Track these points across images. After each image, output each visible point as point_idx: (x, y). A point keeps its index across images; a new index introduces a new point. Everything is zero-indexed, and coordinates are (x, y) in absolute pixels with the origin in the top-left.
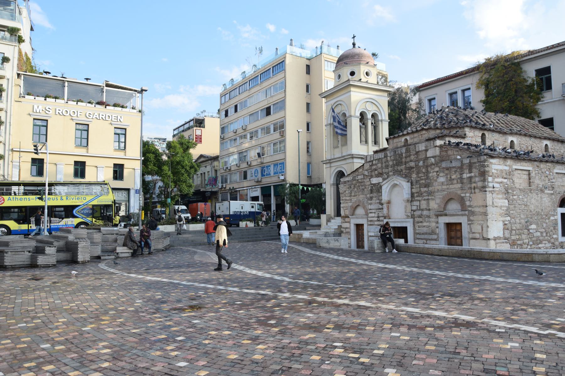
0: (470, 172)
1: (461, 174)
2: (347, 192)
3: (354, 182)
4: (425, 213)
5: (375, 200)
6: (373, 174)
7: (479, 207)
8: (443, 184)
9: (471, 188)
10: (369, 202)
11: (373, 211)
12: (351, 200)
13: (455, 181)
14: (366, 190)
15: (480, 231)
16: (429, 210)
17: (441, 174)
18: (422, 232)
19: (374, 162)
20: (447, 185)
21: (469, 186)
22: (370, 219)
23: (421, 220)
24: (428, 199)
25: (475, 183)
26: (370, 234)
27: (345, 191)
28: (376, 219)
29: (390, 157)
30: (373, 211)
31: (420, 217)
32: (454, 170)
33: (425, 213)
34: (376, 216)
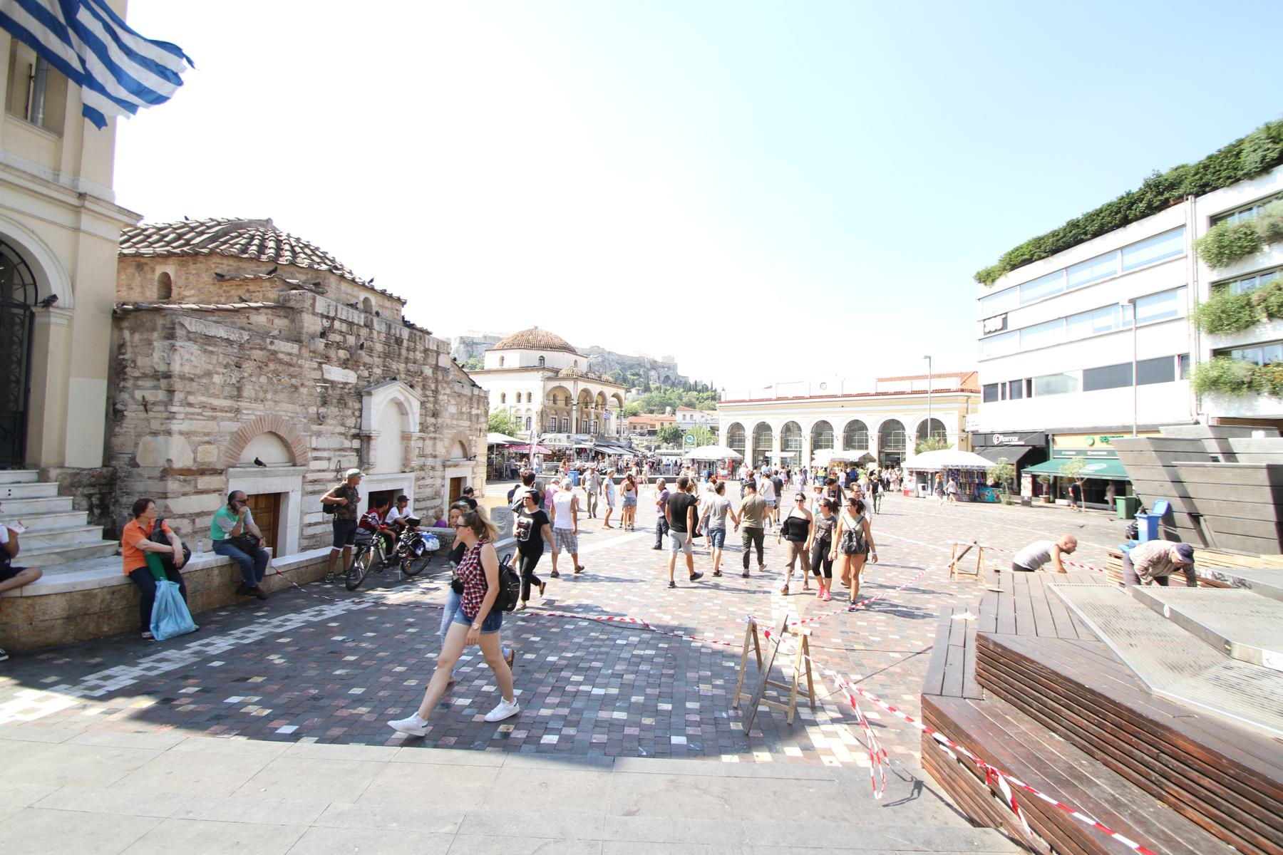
2: (217, 379)
3: (257, 354)
4: (430, 461)
5: (331, 426)
6: (332, 353)
8: (452, 416)
10: (315, 428)
11: (325, 454)
12: (238, 411)
14: (304, 391)
16: (435, 457)
17: (453, 401)
18: (422, 496)
19: (337, 324)
22: (310, 477)
23: (422, 474)
26: (309, 519)
27: (209, 374)
28: (331, 475)
29: (379, 333)
30: (325, 454)
31: (422, 468)
33: (430, 461)
34: (333, 466)
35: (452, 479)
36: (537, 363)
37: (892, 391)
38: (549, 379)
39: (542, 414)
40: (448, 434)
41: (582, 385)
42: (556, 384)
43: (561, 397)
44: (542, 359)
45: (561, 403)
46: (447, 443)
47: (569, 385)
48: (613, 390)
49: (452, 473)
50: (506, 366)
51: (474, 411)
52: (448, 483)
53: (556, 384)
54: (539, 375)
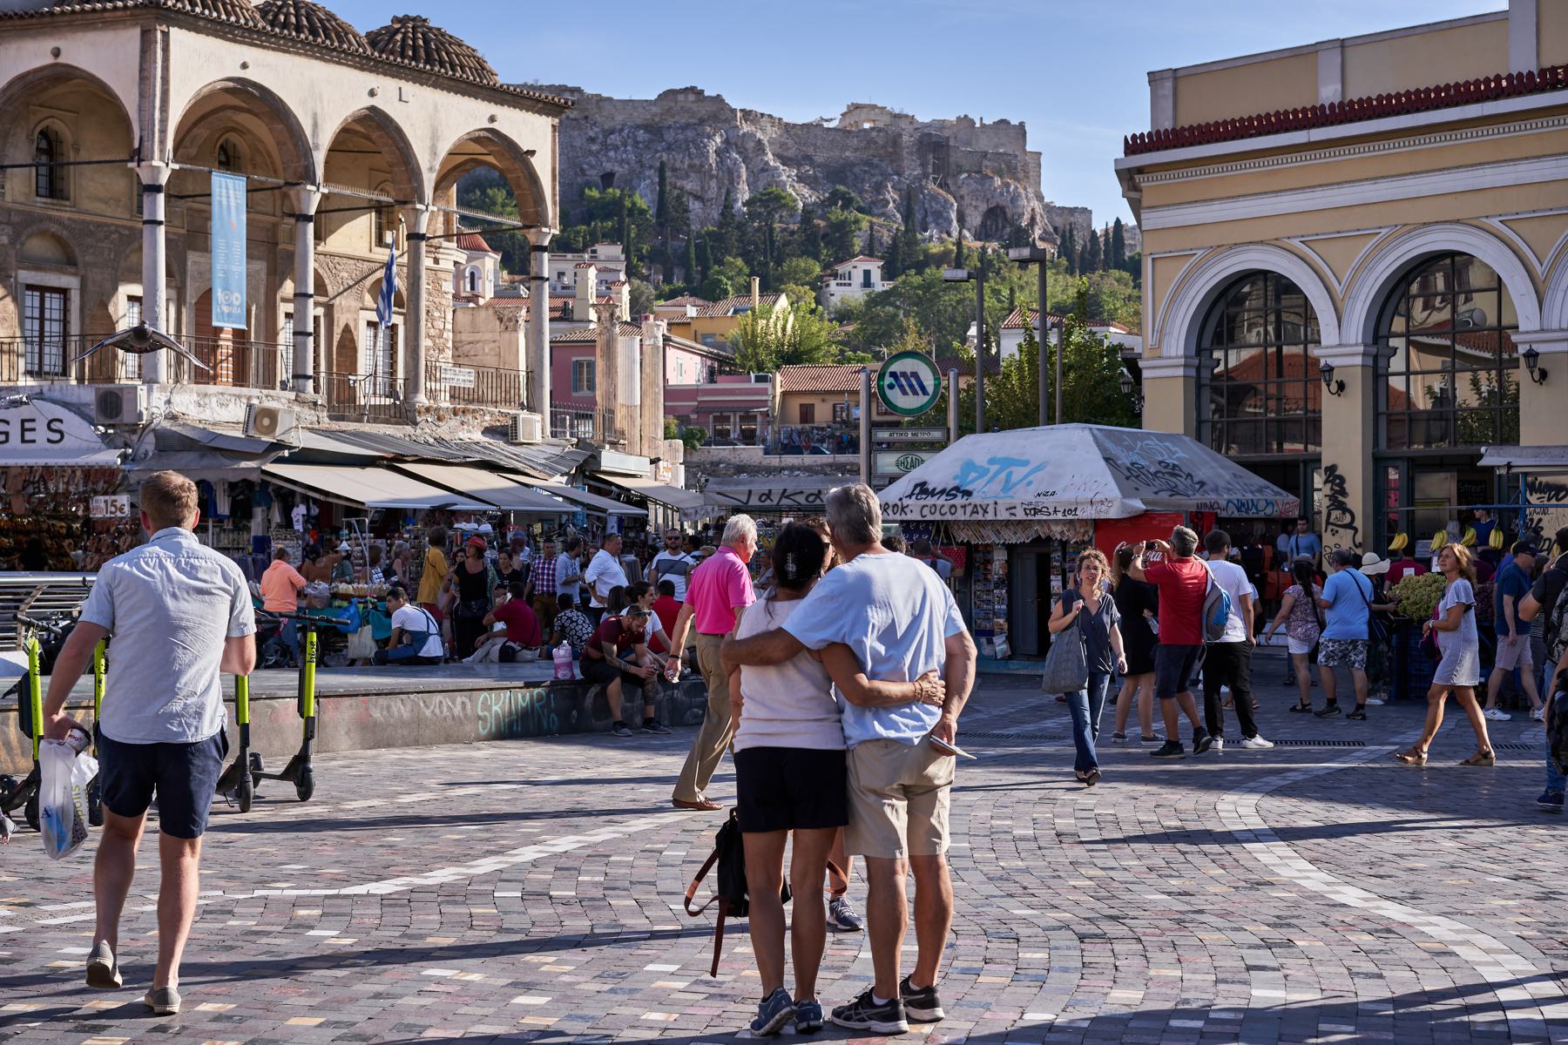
43: (87, 142)
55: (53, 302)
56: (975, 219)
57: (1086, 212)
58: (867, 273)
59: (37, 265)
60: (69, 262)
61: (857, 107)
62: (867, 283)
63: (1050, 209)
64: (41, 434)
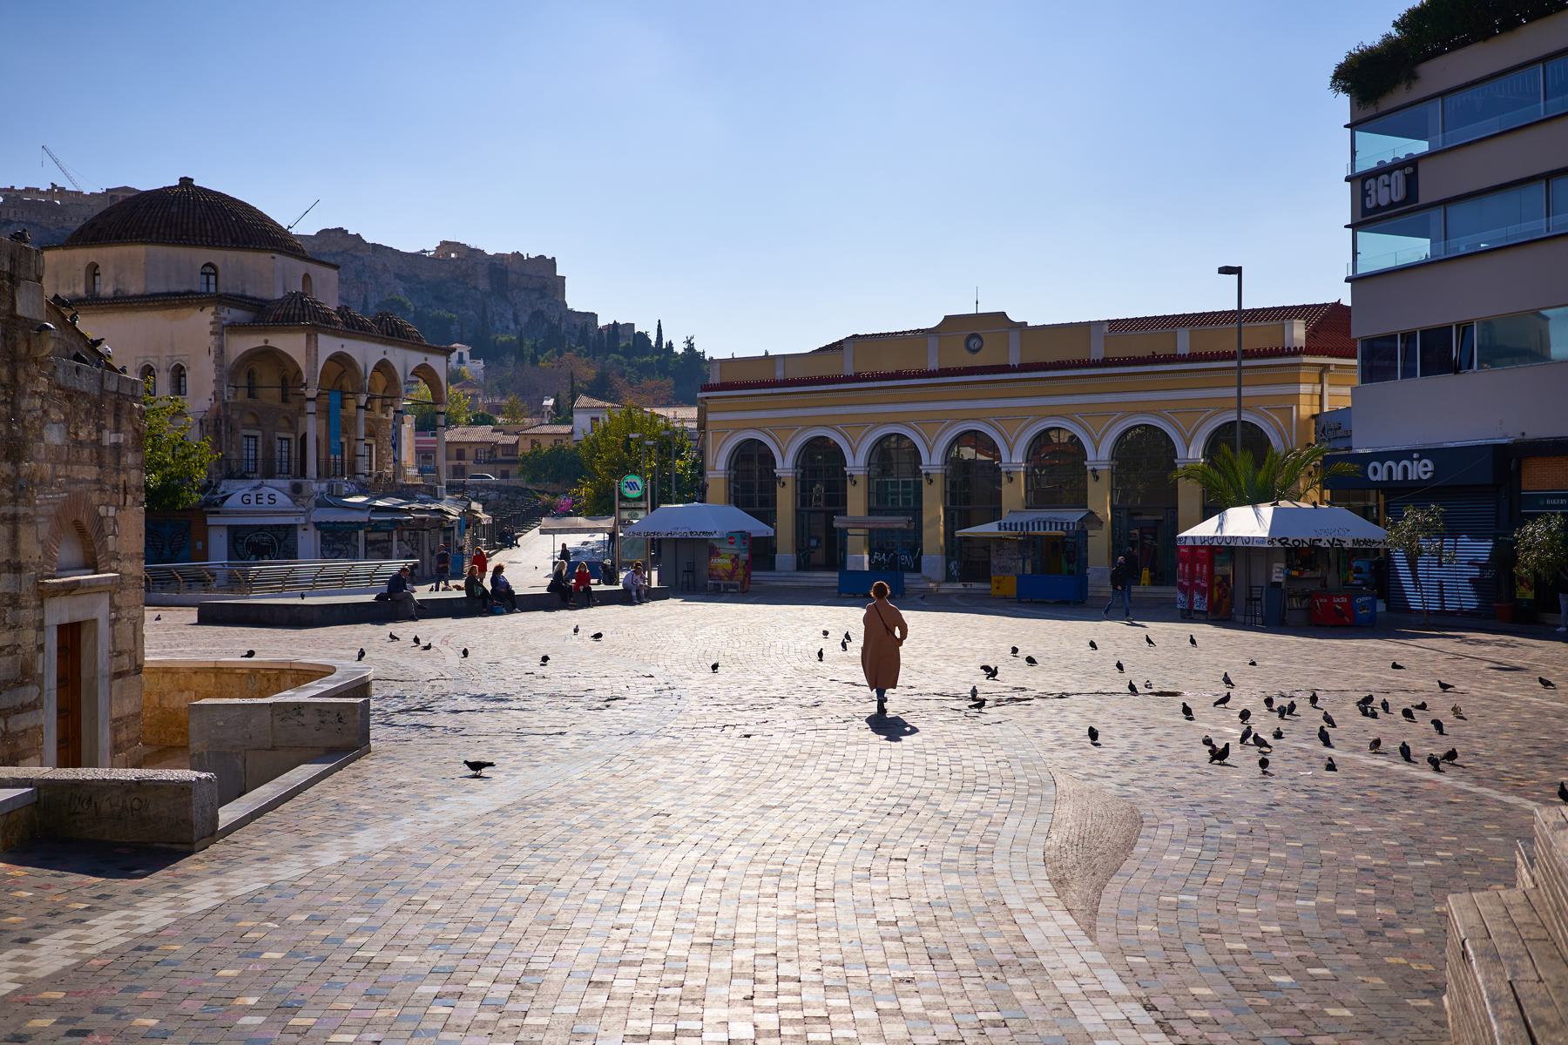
0: (117, 430)
1: (100, 429)
7: (130, 558)
8: (56, 456)
9: (116, 487)
13: (86, 453)
15: (132, 646)
17: (55, 414)
20: (67, 463)
21: (113, 480)
24: (14, 519)
25: (124, 470)
32: (84, 405)
35: (61, 628)
36: (198, 285)
37: (1145, 352)
38: (235, 328)
39: (217, 424)
40: (45, 501)
41: (328, 345)
42: (255, 341)
44: (210, 270)
45: (270, 395)
46: (44, 530)
47: (291, 344)
48: (416, 358)
49: (60, 612)
50: (106, 289)
51: (109, 438)
52: (51, 641)
53: (255, 341)
54: (201, 321)
55: (252, 442)
56: (524, 319)
57: (594, 316)
58: (461, 355)
59: (247, 427)
60: (258, 425)
61: (445, 244)
62: (461, 361)
63: (571, 311)
64: (265, 500)
